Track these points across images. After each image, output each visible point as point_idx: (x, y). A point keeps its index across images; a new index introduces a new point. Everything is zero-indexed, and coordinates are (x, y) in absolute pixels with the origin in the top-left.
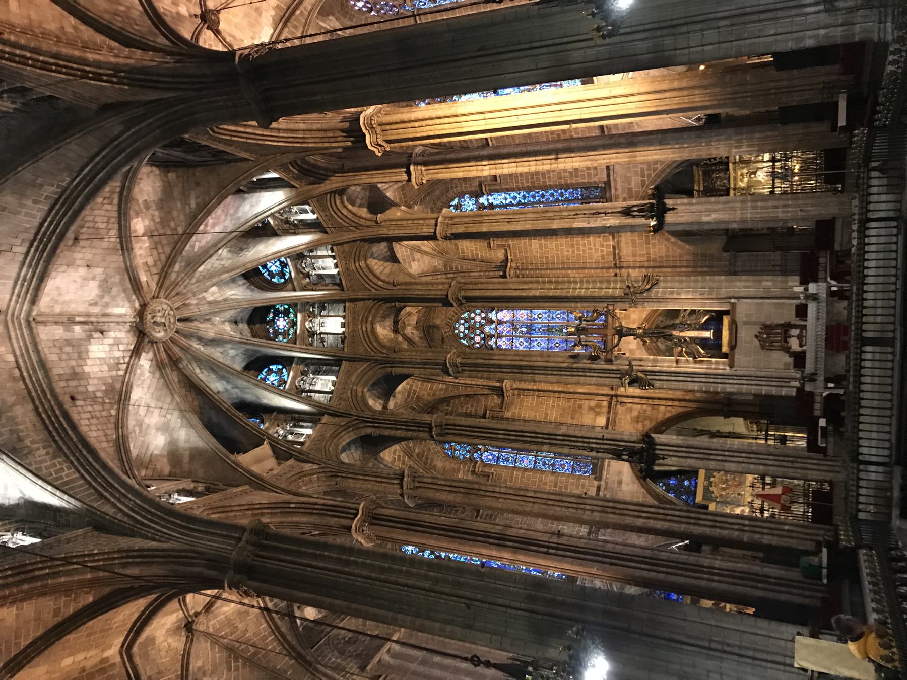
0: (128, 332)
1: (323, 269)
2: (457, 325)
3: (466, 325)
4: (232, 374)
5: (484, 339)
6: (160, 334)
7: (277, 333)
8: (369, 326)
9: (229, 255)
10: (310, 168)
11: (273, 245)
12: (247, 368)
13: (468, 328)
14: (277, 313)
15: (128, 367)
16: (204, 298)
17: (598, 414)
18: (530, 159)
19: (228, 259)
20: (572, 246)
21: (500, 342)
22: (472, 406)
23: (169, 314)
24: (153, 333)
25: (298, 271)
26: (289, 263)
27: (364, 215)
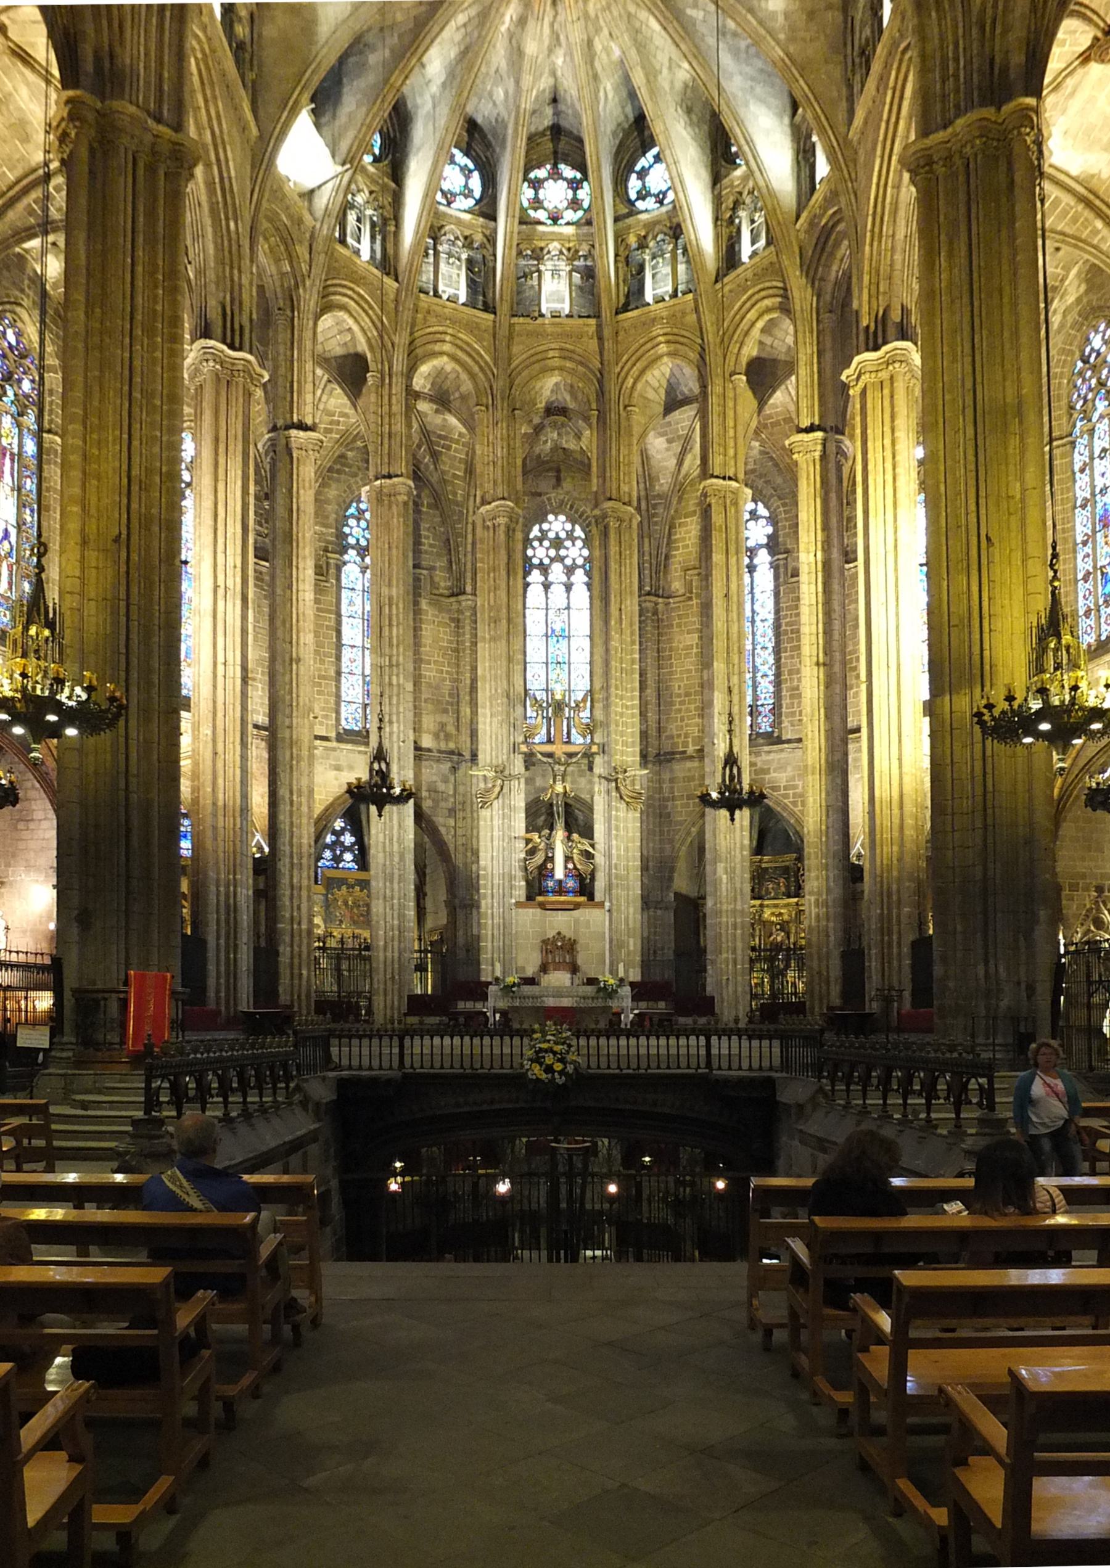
1: (654, 276)
2: (562, 518)
5: (541, 563)
8: (557, 362)
9: (679, 85)
13: (557, 537)
14: (574, 185)
17: (436, 736)
19: (672, 82)
20: (687, 694)
25: (650, 226)
26: (664, 209)
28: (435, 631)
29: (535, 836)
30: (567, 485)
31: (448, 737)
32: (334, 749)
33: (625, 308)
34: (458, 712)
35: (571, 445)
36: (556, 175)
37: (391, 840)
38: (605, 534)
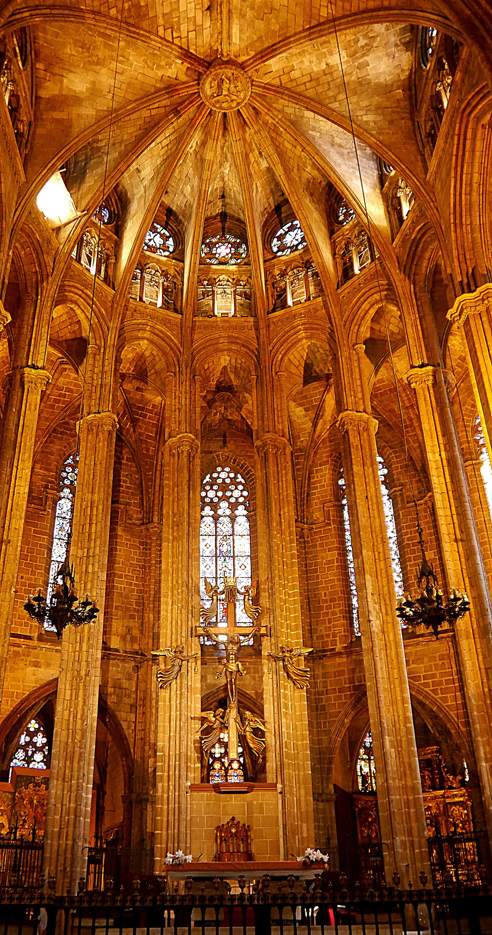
0: (211, 48)
3: (228, 481)
4: (162, 181)
6: (208, 87)
7: (211, 246)
8: (226, 346)
9: (304, 180)
10: (418, 253)
11: (319, 228)
12: (169, 212)
15: (168, 41)
16: (252, 151)
18: (453, 508)
20: (332, 600)
21: (209, 520)
22: (128, 487)
23: (232, 101)
24: (210, 79)
25: (288, 263)
26: (297, 253)
27: (362, 329)
28: (128, 552)
29: (210, 715)
30: (231, 446)
31: (133, 639)
32: (35, 648)
33: (274, 310)
34: (143, 617)
35: (235, 417)
36: (223, 241)
37: (75, 717)
38: (266, 459)
